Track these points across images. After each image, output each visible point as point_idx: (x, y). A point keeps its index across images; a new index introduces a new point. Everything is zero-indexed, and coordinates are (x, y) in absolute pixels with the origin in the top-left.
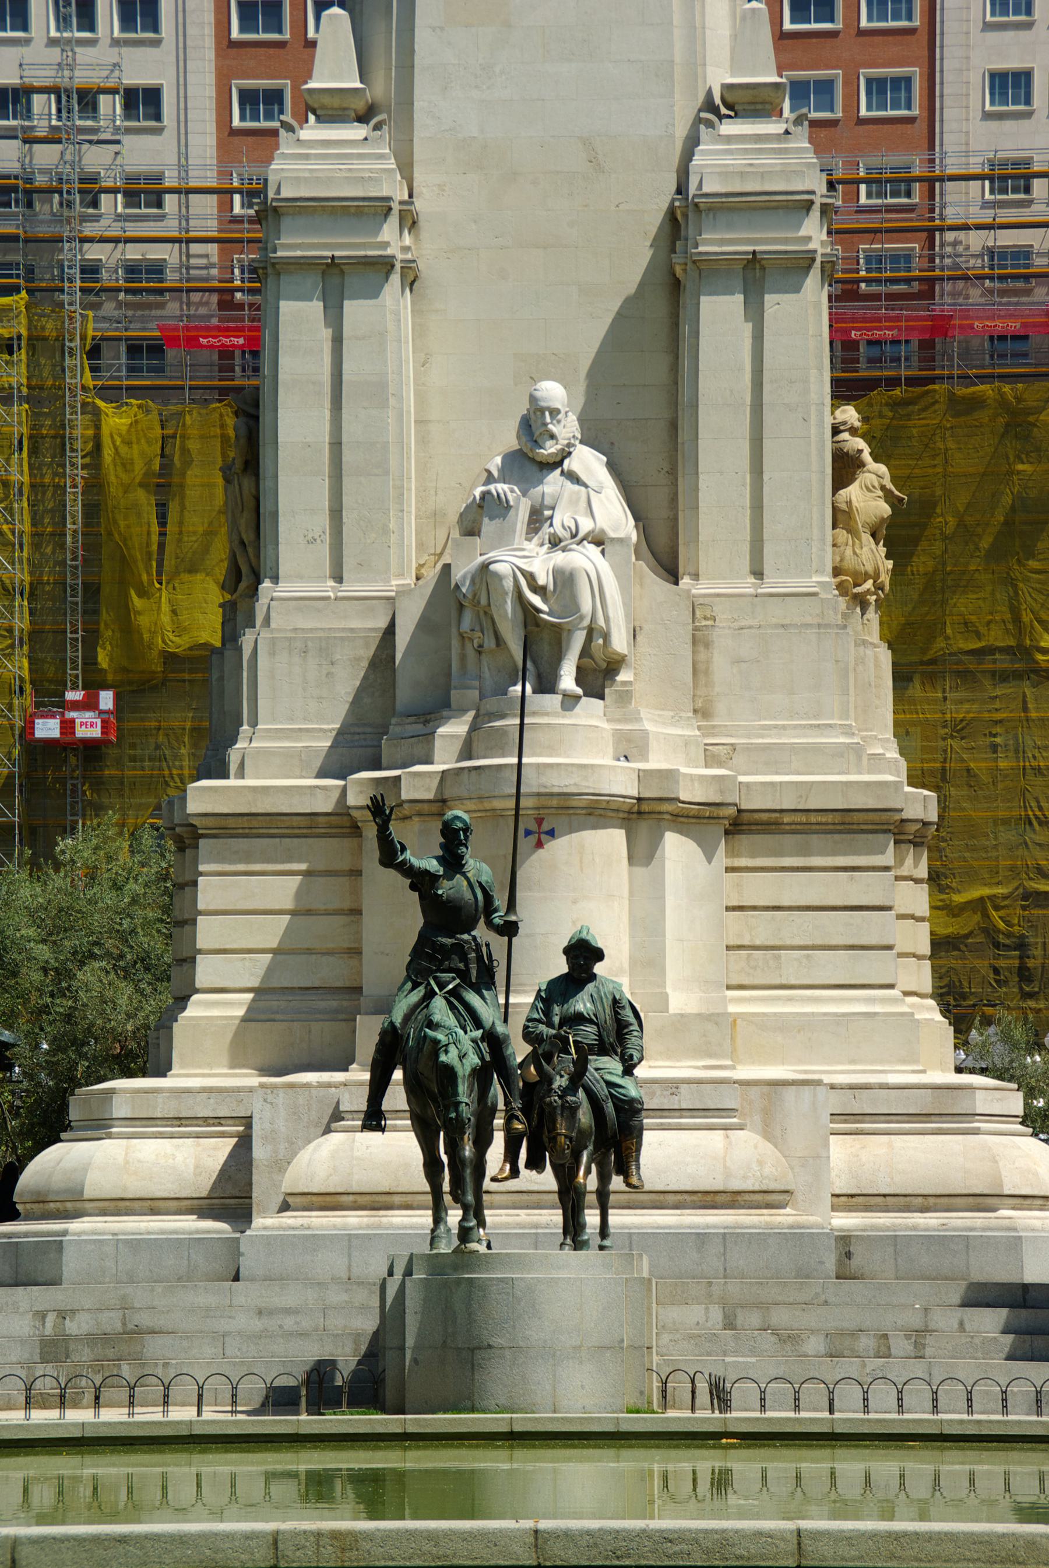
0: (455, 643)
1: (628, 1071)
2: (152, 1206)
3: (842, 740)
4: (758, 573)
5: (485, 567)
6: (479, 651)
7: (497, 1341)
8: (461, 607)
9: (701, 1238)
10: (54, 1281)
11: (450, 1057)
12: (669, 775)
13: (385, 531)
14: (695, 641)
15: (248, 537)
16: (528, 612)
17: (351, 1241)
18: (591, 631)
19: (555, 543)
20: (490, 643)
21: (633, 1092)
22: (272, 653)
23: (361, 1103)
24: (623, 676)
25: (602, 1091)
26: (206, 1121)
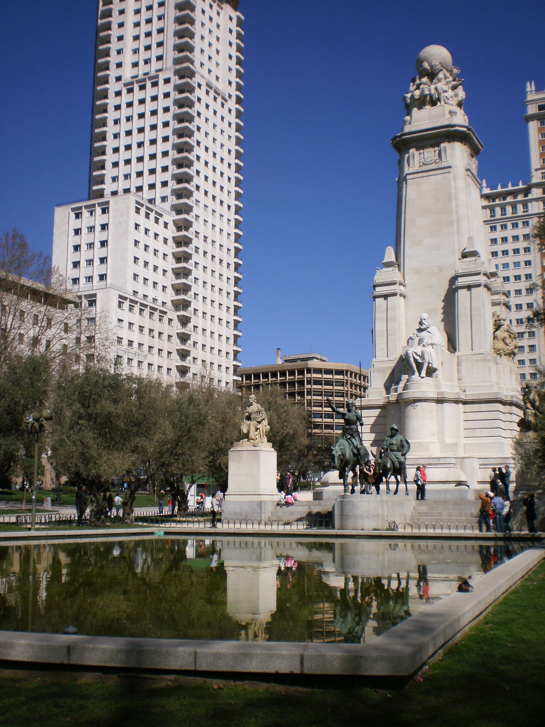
1: (404, 455)
3: (489, 384)
4: (472, 350)
6: (408, 369)
7: (351, 514)
9: (440, 491)
10: (322, 500)
11: (334, 453)
13: (396, 346)
14: (458, 365)
16: (415, 360)
18: (429, 363)
21: (402, 459)
22: (374, 372)
24: (436, 373)
25: (394, 459)
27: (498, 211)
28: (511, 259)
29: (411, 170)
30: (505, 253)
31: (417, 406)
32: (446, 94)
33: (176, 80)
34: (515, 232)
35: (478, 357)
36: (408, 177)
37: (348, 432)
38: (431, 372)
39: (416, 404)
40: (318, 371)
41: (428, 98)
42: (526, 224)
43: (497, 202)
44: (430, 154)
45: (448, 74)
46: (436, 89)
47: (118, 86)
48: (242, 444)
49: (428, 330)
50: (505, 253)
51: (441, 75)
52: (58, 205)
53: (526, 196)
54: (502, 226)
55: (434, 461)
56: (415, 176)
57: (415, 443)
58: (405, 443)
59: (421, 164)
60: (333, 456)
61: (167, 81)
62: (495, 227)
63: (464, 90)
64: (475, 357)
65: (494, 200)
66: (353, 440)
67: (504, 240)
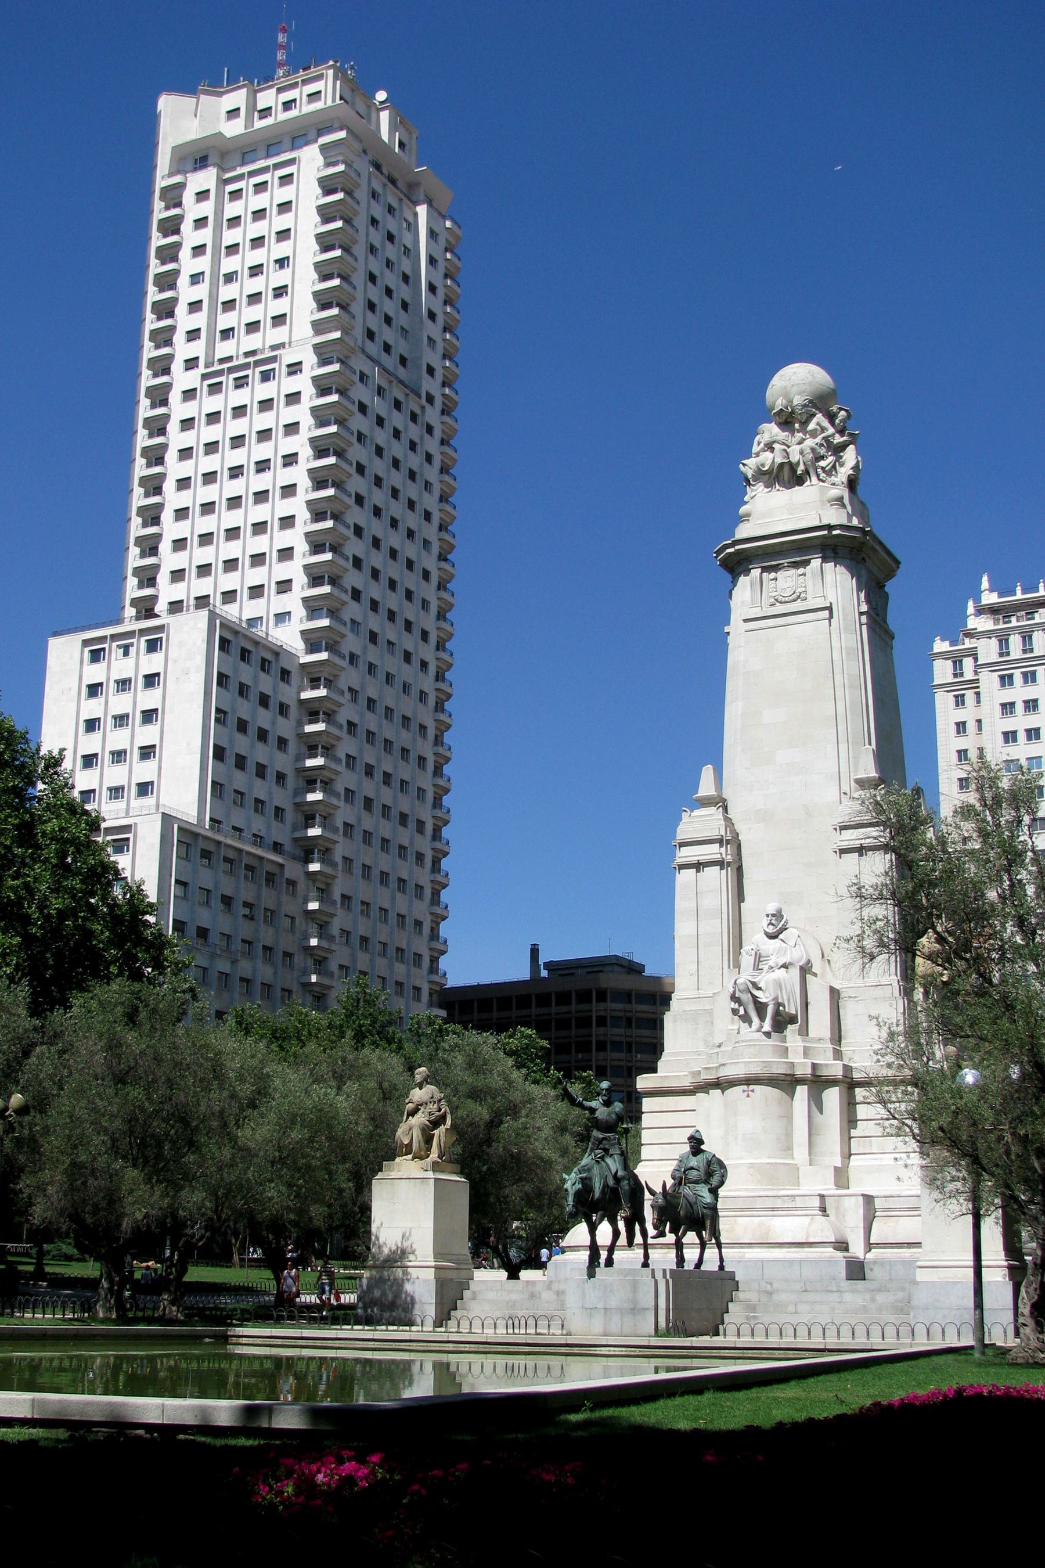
1: (714, 1191)
5: (735, 983)
9: (790, 1263)
16: (754, 997)
20: (742, 1012)
27: (1015, 642)
31: (753, 1091)
32: (822, 463)
33: (311, 368)
35: (879, 992)
37: (601, 1146)
39: (751, 1087)
40: (627, 996)
41: (786, 470)
43: (1014, 622)
44: (787, 580)
45: (826, 423)
47: (189, 379)
48: (399, 1165)
49: (781, 936)
51: (812, 426)
52: (56, 634)
54: (1025, 675)
55: (784, 1202)
57: (737, 1166)
58: (715, 1167)
59: (772, 600)
60: (566, 1190)
61: (295, 368)
62: (1011, 676)
63: (858, 453)
65: (1007, 618)
66: (609, 1160)
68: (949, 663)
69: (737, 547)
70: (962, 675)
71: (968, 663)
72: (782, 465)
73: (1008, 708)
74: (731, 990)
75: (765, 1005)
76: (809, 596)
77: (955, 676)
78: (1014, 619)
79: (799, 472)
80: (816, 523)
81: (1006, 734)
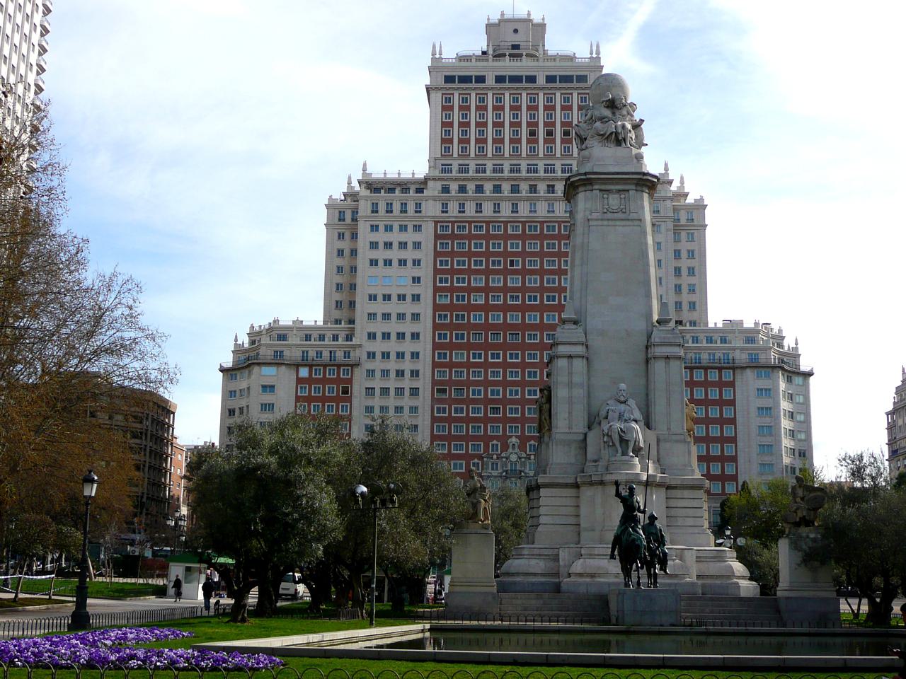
0: (602, 443)
2: (535, 574)
5: (611, 426)
8: (604, 435)
9: (670, 585)
12: (655, 476)
15: (547, 418)
16: (620, 437)
17: (587, 584)
19: (626, 420)
20: (611, 444)
22: (557, 445)
23: (609, 551)
26: (546, 555)
28: (395, 269)
29: (595, 215)
30: (388, 263)
34: (403, 237)
35: (678, 437)
36: (591, 223)
38: (637, 451)
42: (417, 228)
44: (614, 201)
46: (623, 126)
50: (388, 263)
53: (420, 191)
56: (600, 223)
64: (674, 437)
65: (377, 190)
67: (388, 245)
68: (337, 212)
69: (588, 176)
70: (344, 220)
71: (348, 216)
72: (612, 133)
73: (374, 245)
74: (606, 431)
75: (628, 441)
76: (628, 212)
77: (340, 220)
78: (382, 191)
79: (620, 138)
80: (633, 170)
81: (371, 261)
